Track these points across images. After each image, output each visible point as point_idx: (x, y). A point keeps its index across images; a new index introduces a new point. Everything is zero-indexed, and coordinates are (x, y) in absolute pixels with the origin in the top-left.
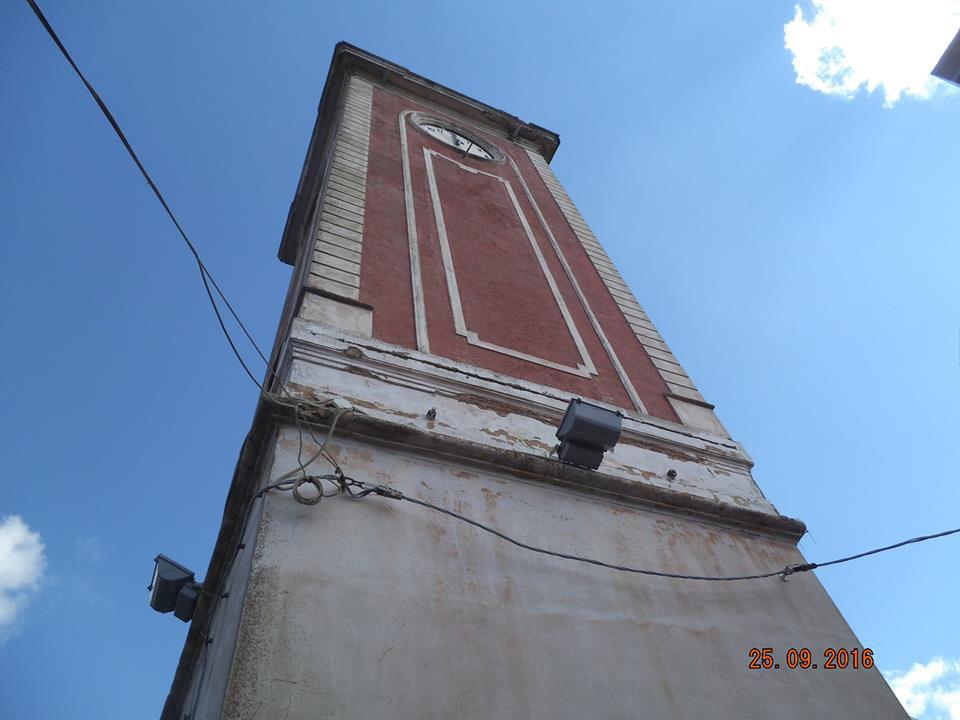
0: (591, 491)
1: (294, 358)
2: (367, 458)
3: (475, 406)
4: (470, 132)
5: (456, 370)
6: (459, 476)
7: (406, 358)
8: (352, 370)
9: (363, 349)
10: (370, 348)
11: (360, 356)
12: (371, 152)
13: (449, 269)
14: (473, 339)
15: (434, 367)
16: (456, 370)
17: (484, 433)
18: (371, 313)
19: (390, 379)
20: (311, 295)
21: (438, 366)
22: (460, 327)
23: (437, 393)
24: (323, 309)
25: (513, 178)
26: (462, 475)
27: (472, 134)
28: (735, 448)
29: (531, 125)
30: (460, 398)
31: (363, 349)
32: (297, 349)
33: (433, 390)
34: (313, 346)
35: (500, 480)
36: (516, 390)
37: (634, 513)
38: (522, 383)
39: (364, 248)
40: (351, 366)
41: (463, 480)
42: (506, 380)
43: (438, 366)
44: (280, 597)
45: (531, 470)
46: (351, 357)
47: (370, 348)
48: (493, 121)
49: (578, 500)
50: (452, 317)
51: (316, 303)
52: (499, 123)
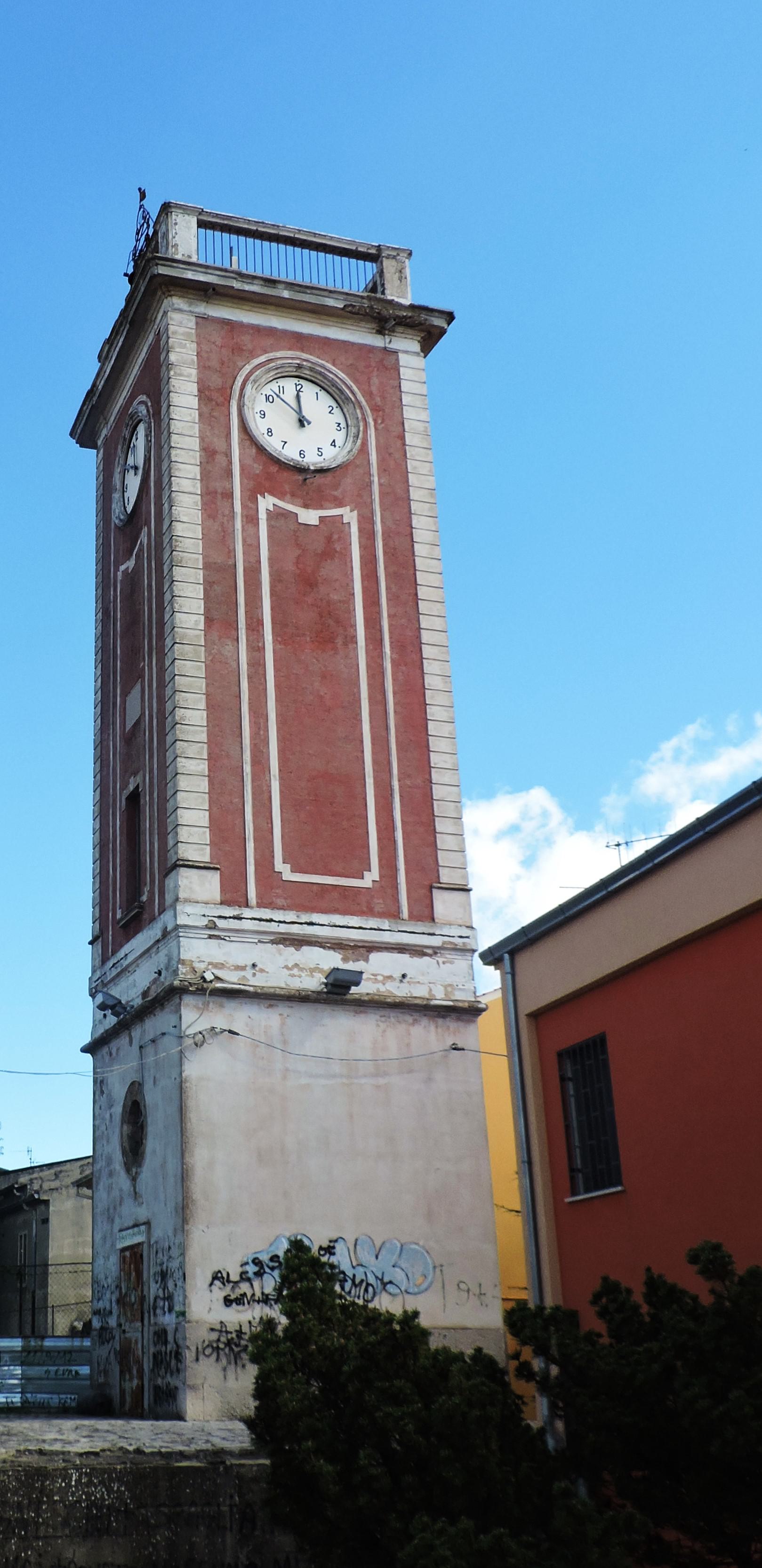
0: (342, 1004)
1: (179, 937)
2: (222, 1006)
3: (281, 946)
4: (320, 373)
5: (271, 920)
6: (268, 1008)
8: (211, 937)
9: (215, 920)
10: (220, 917)
11: (214, 927)
12: (207, 566)
13: (276, 780)
15: (258, 922)
16: (271, 920)
18: (219, 872)
19: (232, 939)
20: (182, 869)
21: (260, 920)
22: (279, 865)
23: (260, 941)
24: (190, 882)
26: (271, 1006)
27: (325, 377)
29: (412, 307)
30: (273, 942)
31: (215, 920)
33: (256, 941)
35: (290, 1005)
36: (311, 927)
38: (316, 918)
39: (211, 783)
41: (270, 1010)
42: (305, 918)
43: (260, 920)
44: (194, 1088)
45: (308, 999)
46: (210, 928)
47: (220, 917)
48: (358, 314)
49: (333, 1010)
50: (273, 851)
51: (187, 878)
52: (366, 314)
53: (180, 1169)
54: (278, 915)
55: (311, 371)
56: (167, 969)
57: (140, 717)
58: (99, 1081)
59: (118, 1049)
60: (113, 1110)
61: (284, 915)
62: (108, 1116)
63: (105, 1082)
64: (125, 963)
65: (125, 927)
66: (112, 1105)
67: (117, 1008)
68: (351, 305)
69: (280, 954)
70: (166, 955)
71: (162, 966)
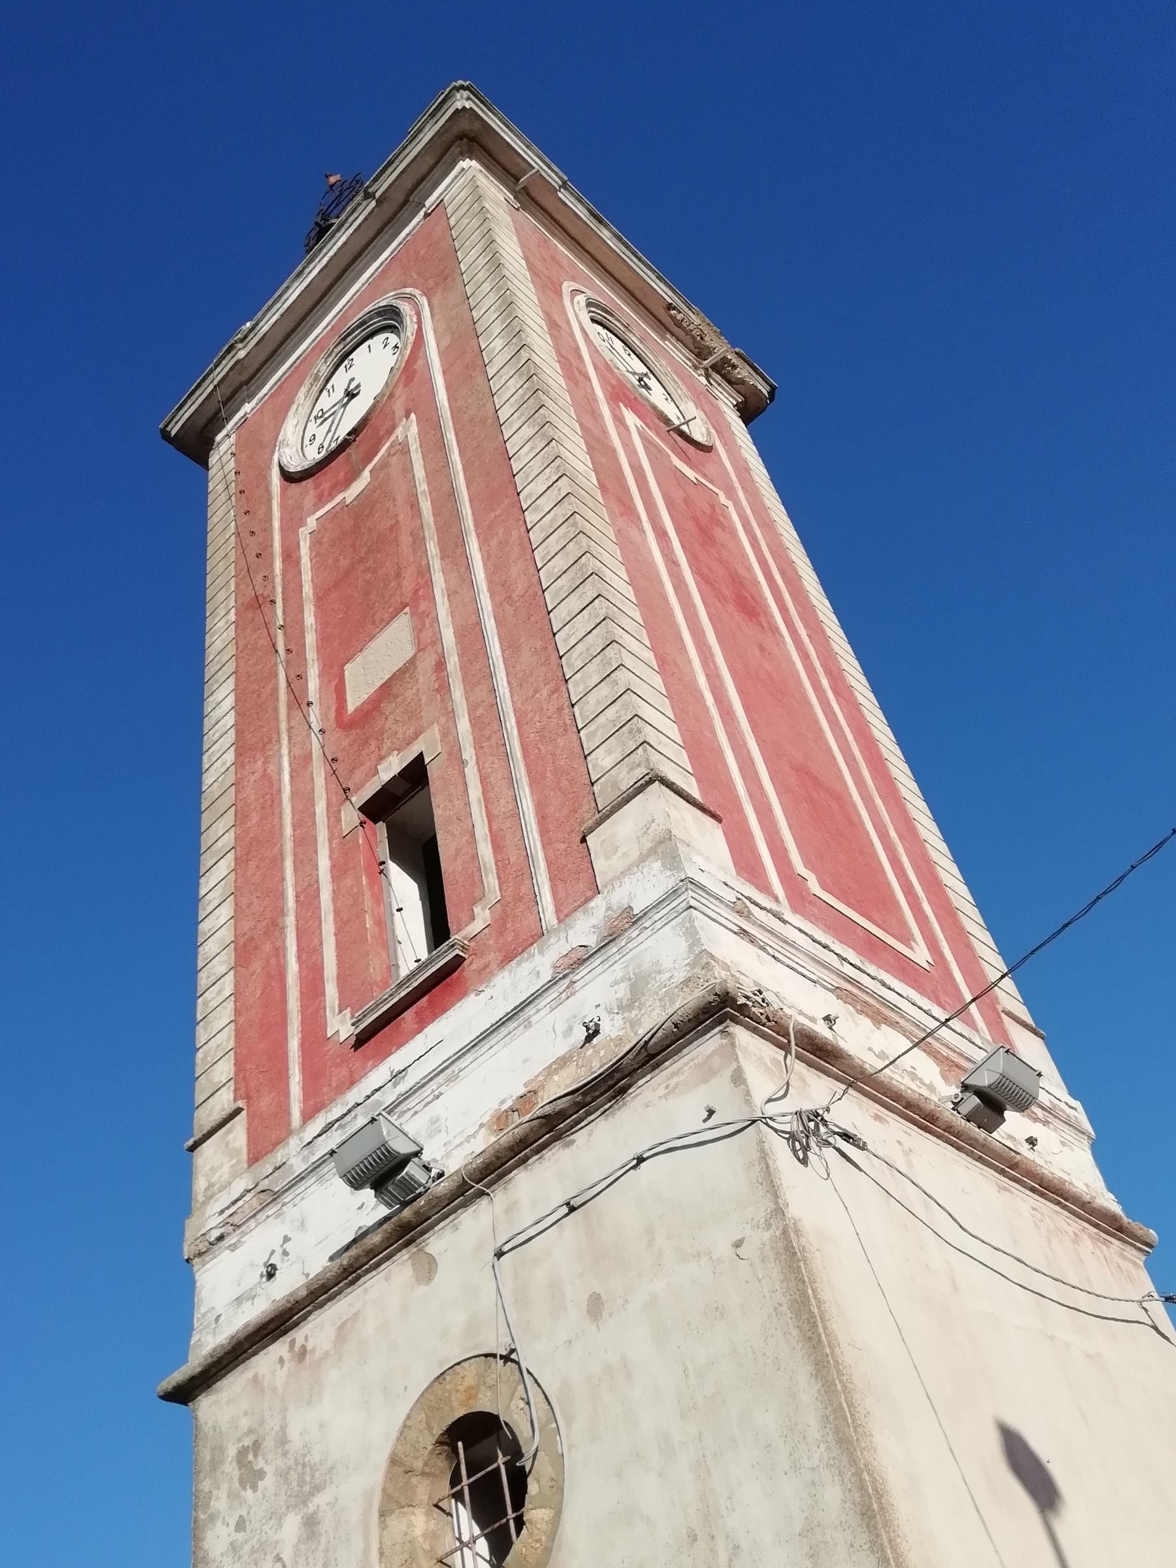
7: (785, 922)
8: (743, 933)
11: (748, 916)
14: (814, 886)
17: (871, 1052)
19: (777, 955)
25: (730, 492)
28: (1075, 1109)
32: (695, 895)
34: (708, 893)
37: (1011, 1192)
40: (741, 928)
42: (871, 969)
53: (833, 1495)
54: (837, 947)
55: (641, 342)
56: (623, 1007)
57: (412, 661)
58: (232, 1451)
59: (343, 1331)
60: (320, 1501)
61: (843, 948)
62: (292, 1525)
63: (269, 1443)
64: (389, 1096)
65: (361, 1040)
66: (317, 1489)
67: (412, 1169)
68: (675, 308)
69: (855, 1022)
70: (616, 983)
71: (591, 1015)
